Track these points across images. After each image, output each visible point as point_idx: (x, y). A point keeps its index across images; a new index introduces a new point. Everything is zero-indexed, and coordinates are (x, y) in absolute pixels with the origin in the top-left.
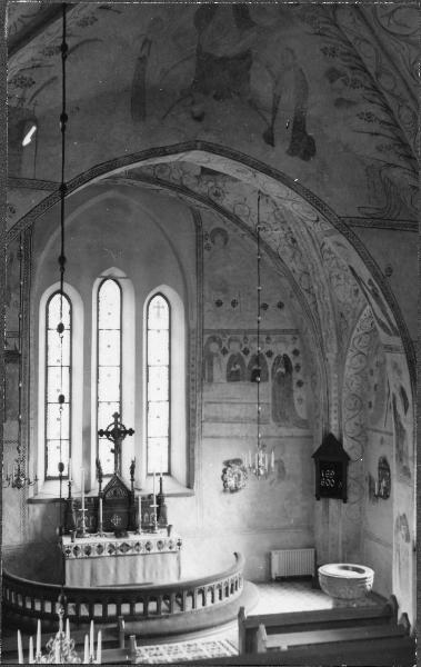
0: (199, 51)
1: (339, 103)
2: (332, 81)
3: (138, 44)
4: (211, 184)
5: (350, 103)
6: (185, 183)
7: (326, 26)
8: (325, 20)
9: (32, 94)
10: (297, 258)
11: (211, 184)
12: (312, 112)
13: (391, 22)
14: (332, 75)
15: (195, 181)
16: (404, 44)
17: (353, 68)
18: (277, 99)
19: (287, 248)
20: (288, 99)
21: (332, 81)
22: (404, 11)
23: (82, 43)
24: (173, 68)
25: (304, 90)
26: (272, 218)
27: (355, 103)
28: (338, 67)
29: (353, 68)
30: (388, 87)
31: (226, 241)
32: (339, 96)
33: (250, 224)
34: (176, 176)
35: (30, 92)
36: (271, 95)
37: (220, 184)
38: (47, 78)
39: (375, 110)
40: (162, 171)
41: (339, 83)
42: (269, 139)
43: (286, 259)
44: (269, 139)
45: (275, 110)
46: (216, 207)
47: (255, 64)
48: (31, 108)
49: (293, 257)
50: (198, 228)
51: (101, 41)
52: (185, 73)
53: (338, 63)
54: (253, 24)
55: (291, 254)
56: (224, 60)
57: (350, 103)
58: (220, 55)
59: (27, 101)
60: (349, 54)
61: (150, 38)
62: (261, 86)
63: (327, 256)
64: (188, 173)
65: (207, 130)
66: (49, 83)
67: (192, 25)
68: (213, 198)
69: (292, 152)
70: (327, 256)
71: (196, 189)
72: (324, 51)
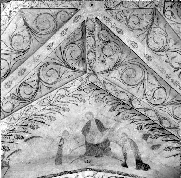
0: (86, 143)
1: (153, 148)
2: (146, 140)
3: (59, 139)
5: (158, 146)
7: (133, 117)
8: (132, 115)
9: (9, 155)
12: (143, 156)
13: (155, 100)
14: (145, 137)
16: (164, 107)
17: (152, 130)
18: (125, 155)
20: (130, 153)
21: (146, 140)
22: (157, 91)
23: (33, 137)
24: (75, 149)
25: (135, 145)
27: (160, 145)
28: (146, 133)
29: (152, 130)
30: (168, 126)
32: (152, 145)
35: (7, 153)
36: (122, 154)
38: (15, 149)
39: (170, 144)
41: (149, 139)
42: (125, 165)
44: (125, 165)
45: (125, 158)
47: (111, 143)
48: (7, 161)
51: (41, 137)
52: (82, 150)
53: (146, 131)
54: (106, 129)
56: (97, 145)
57: (158, 146)
58: (95, 143)
59: (6, 158)
60: (148, 125)
61: (63, 137)
62: (116, 150)
65: (92, 165)
66: (16, 151)
67: (81, 133)
69: (138, 168)
72: (138, 128)
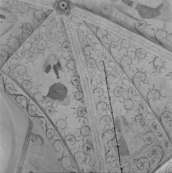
4: (49, 104)
6: (35, 97)
10: (87, 161)
11: (49, 104)
15: (41, 98)
19: (82, 155)
26: (79, 132)
31: (42, 144)
33: (63, 135)
34: (33, 91)
37: (54, 106)
40: (27, 85)
43: (79, 161)
46: (48, 117)
49: (85, 160)
50: (30, 128)
55: (83, 159)
63: (109, 159)
64: (40, 93)
68: (47, 112)
70: (109, 159)
71: (40, 104)
